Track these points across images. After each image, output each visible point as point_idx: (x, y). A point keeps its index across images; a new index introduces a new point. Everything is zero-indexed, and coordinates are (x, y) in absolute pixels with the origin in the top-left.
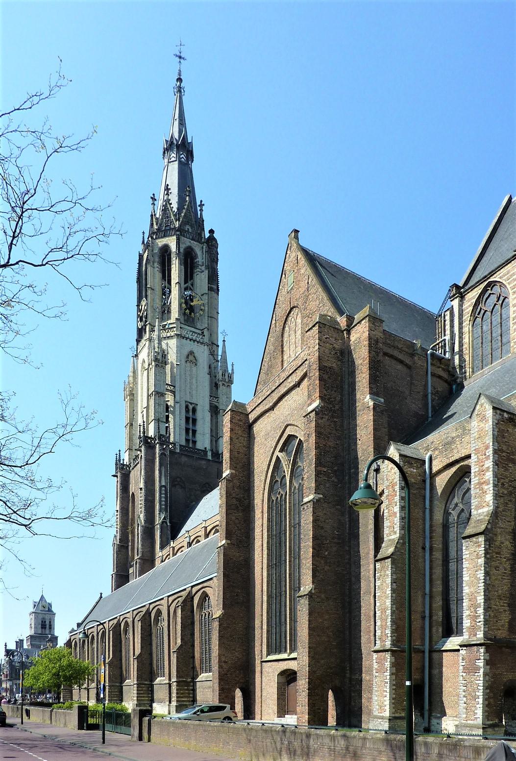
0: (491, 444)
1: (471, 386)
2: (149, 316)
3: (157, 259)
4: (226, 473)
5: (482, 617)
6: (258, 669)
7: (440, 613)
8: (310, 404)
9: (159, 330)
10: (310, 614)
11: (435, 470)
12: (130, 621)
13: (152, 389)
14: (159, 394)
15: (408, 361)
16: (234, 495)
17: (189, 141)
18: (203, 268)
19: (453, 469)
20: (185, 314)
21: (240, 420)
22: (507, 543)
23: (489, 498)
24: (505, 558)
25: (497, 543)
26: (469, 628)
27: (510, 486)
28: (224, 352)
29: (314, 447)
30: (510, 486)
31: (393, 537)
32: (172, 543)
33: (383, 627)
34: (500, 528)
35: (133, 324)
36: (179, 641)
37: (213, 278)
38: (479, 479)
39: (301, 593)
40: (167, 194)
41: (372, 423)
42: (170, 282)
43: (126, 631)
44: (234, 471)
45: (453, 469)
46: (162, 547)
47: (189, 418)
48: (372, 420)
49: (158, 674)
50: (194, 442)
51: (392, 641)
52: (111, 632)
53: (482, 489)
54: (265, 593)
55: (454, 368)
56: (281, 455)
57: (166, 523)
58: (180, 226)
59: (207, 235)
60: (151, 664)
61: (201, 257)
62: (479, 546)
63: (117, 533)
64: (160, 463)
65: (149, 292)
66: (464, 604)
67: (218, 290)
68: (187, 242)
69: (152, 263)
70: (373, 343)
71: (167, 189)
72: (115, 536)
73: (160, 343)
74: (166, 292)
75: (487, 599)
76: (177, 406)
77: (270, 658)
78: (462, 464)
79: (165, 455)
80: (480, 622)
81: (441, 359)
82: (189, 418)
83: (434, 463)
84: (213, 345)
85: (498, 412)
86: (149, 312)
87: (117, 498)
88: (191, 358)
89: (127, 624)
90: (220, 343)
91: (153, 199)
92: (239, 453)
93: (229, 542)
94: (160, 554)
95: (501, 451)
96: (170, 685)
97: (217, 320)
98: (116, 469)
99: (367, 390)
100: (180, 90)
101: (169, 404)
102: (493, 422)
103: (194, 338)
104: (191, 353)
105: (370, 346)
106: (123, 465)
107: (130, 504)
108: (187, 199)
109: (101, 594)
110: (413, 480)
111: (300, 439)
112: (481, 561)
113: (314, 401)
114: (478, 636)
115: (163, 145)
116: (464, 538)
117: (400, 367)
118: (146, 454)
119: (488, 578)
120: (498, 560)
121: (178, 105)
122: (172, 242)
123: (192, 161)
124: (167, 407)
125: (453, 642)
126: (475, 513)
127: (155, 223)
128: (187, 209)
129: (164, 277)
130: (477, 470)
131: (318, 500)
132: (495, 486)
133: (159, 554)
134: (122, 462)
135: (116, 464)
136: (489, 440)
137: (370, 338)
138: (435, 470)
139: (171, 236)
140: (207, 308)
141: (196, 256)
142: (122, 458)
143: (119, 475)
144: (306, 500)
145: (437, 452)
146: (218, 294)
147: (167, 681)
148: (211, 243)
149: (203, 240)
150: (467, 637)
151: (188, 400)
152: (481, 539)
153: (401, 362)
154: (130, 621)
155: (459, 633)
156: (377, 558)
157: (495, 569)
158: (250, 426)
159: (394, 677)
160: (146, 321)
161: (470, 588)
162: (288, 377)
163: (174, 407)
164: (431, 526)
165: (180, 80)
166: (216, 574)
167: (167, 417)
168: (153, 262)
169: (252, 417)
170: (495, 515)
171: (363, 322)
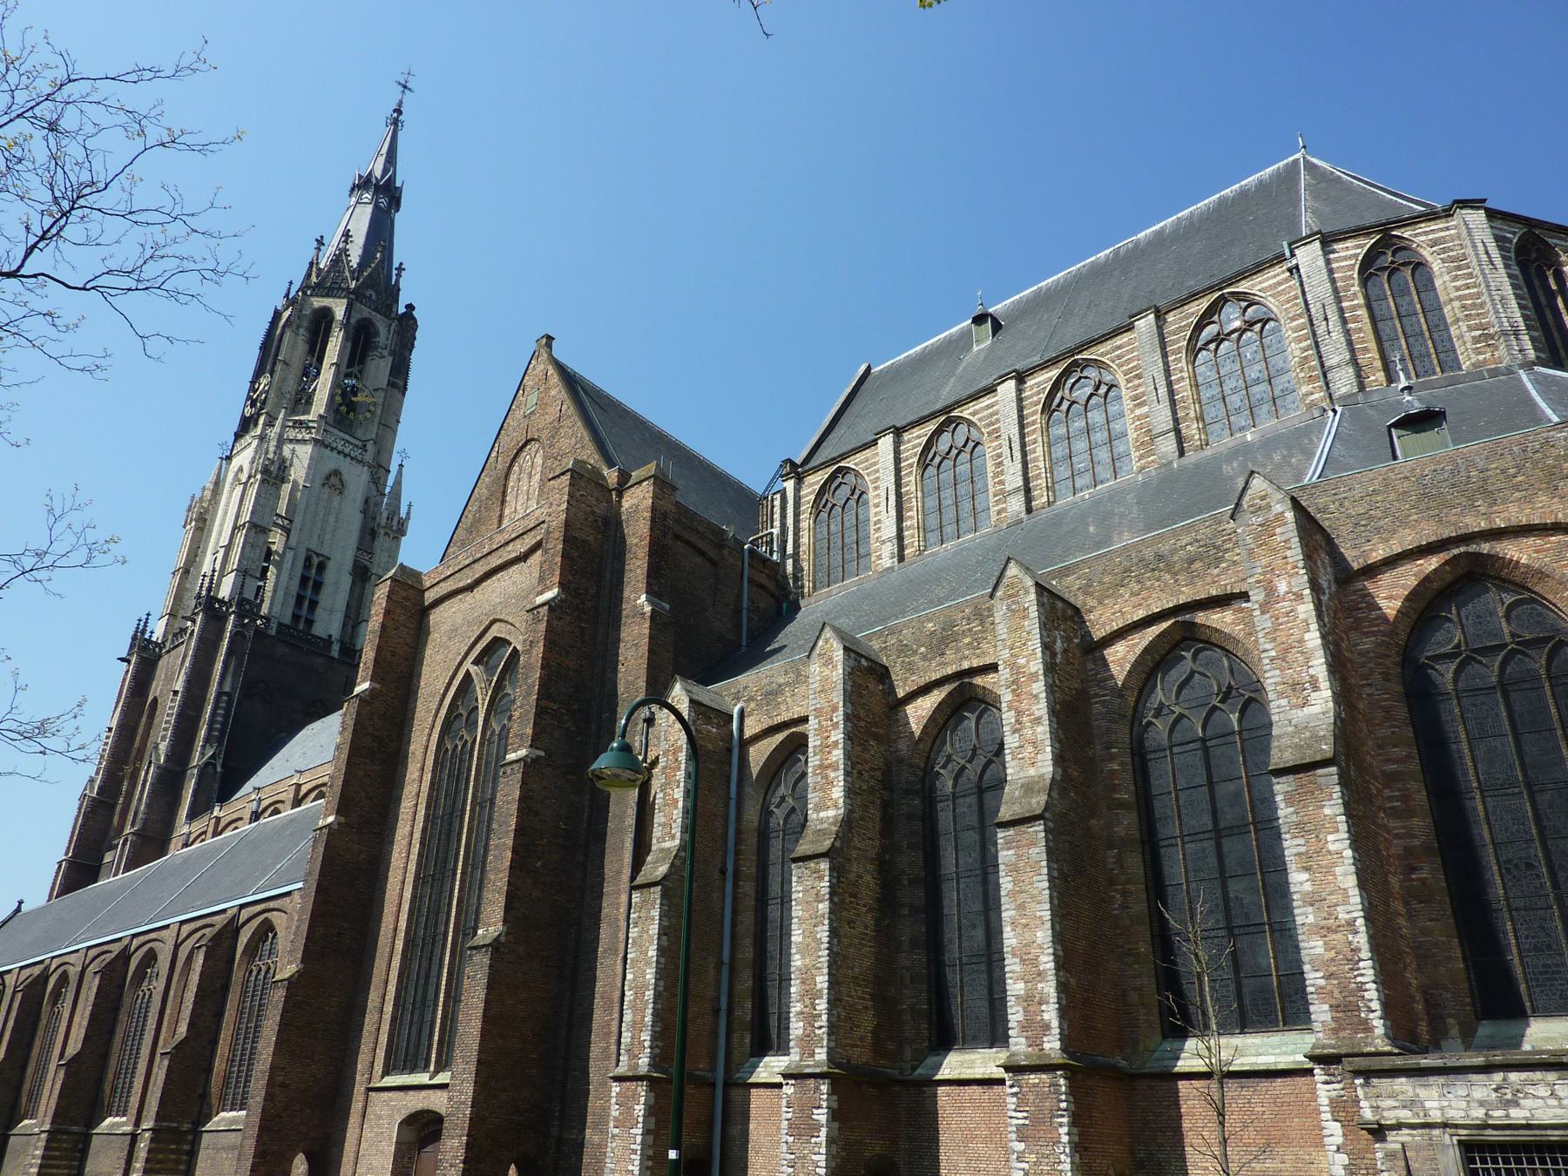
0: (841, 704)
1: (813, 607)
2: (270, 402)
3: (305, 324)
4: (362, 687)
5: (824, 1017)
6: (357, 1105)
7: (749, 1005)
8: (541, 593)
9: (284, 427)
10: (490, 987)
11: (748, 733)
12: (73, 972)
13: (246, 517)
14: (257, 528)
15: (712, 553)
16: (370, 730)
17: (398, 184)
18: (385, 353)
19: (780, 737)
20: (337, 411)
21: (405, 598)
22: (868, 878)
23: (838, 793)
24: (864, 906)
25: (852, 876)
26: (800, 1039)
27: (872, 777)
28: (398, 482)
29: (539, 664)
30: (872, 777)
31: (667, 844)
32: (217, 809)
33: (637, 1026)
34: (855, 848)
35: (236, 407)
36: (183, 1029)
37: (400, 371)
38: (821, 760)
39: (478, 941)
40: (346, 242)
41: (647, 640)
42: (320, 360)
43: (57, 995)
44: (377, 686)
45: (780, 737)
46: (193, 816)
47: (309, 578)
48: (647, 634)
49: (110, 1106)
50: (310, 622)
51: (653, 1057)
52: (19, 996)
53: (827, 777)
54: (401, 935)
55: (785, 577)
56: (474, 669)
57: (215, 766)
58: (357, 288)
59: (402, 310)
60: (100, 1081)
61: (385, 333)
62: (821, 878)
63: (97, 773)
64: (229, 648)
65: (279, 367)
66: (793, 990)
67: (406, 389)
68: (364, 312)
69: (294, 327)
70: (658, 518)
71: (347, 235)
72: (92, 781)
73: (279, 446)
74: (310, 371)
75: (834, 983)
76: (290, 554)
77: (390, 1081)
78: (794, 730)
79: (244, 636)
80: (820, 1028)
81: (765, 561)
82: (309, 578)
83: (748, 721)
84: (379, 469)
85: (852, 655)
86: (272, 395)
87: (117, 703)
88: (334, 480)
89: (64, 978)
90: (394, 468)
92: (393, 654)
93: (342, 820)
94: (185, 830)
95: (859, 718)
96: (134, 1138)
97: (395, 432)
98: (132, 646)
99: (643, 586)
100: (396, 122)
101: (274, 548)
102: (844, 670)
103: (347, 451)
104: (336, 473)
105: (653, 519)
106: (149, 641)
107: (144, 719)
108: (378, 255)
109: (21, 903)
110: (710, 746)
111: (515, 647)
112: (824, 907)
113: (549, 588)
114: (817, 1057)
115: (352, 178)
116: (795, 860)
117: (699, 560)
118: (203, 630)
119: (835, 941)
120: (854, 909)
121: (388, 139)
122: (339, 308)
123: (397, 210)
124: (269, 553)
125: (770, 1067)
126: (815, 816)
127: (314, 274)
128: (375, 269)
129: (311, 351)
130: (818, 743)
131: (536, 761)
132: (847, 774)
133: (182, 828)
134: (147, 636)
135: (134, 638)
136: (838, 698)
137: (654, 509)
138: (748, 733)
139: (339, 297)
140: (379, 411)
141: (377, 334)
142: (149, 629)
143: (134, 660)
144: (511, 756)
145: (753, 705)
146: (404, 395)
147: (128, 1129)
148: (407, 324)
149: (393, 315)
150: (798, 1058)
151: (313, 547)
152: (824, 865)
153: (702, 553)
154: (73, 972)
155: (783, 1049)
156: (636, 883)
157: (849, 924)
158: (424, 612)
159: (650, 1139)
160: (262, 409)
161: (803, 957)
162: (507, 543)
163: (282, 556)
164: (738, 832)
166: (300, 885)
167: (265, 570)
168: (298, 327)
169: (430, 597)
170: (848, 824)
171: (645, 484)
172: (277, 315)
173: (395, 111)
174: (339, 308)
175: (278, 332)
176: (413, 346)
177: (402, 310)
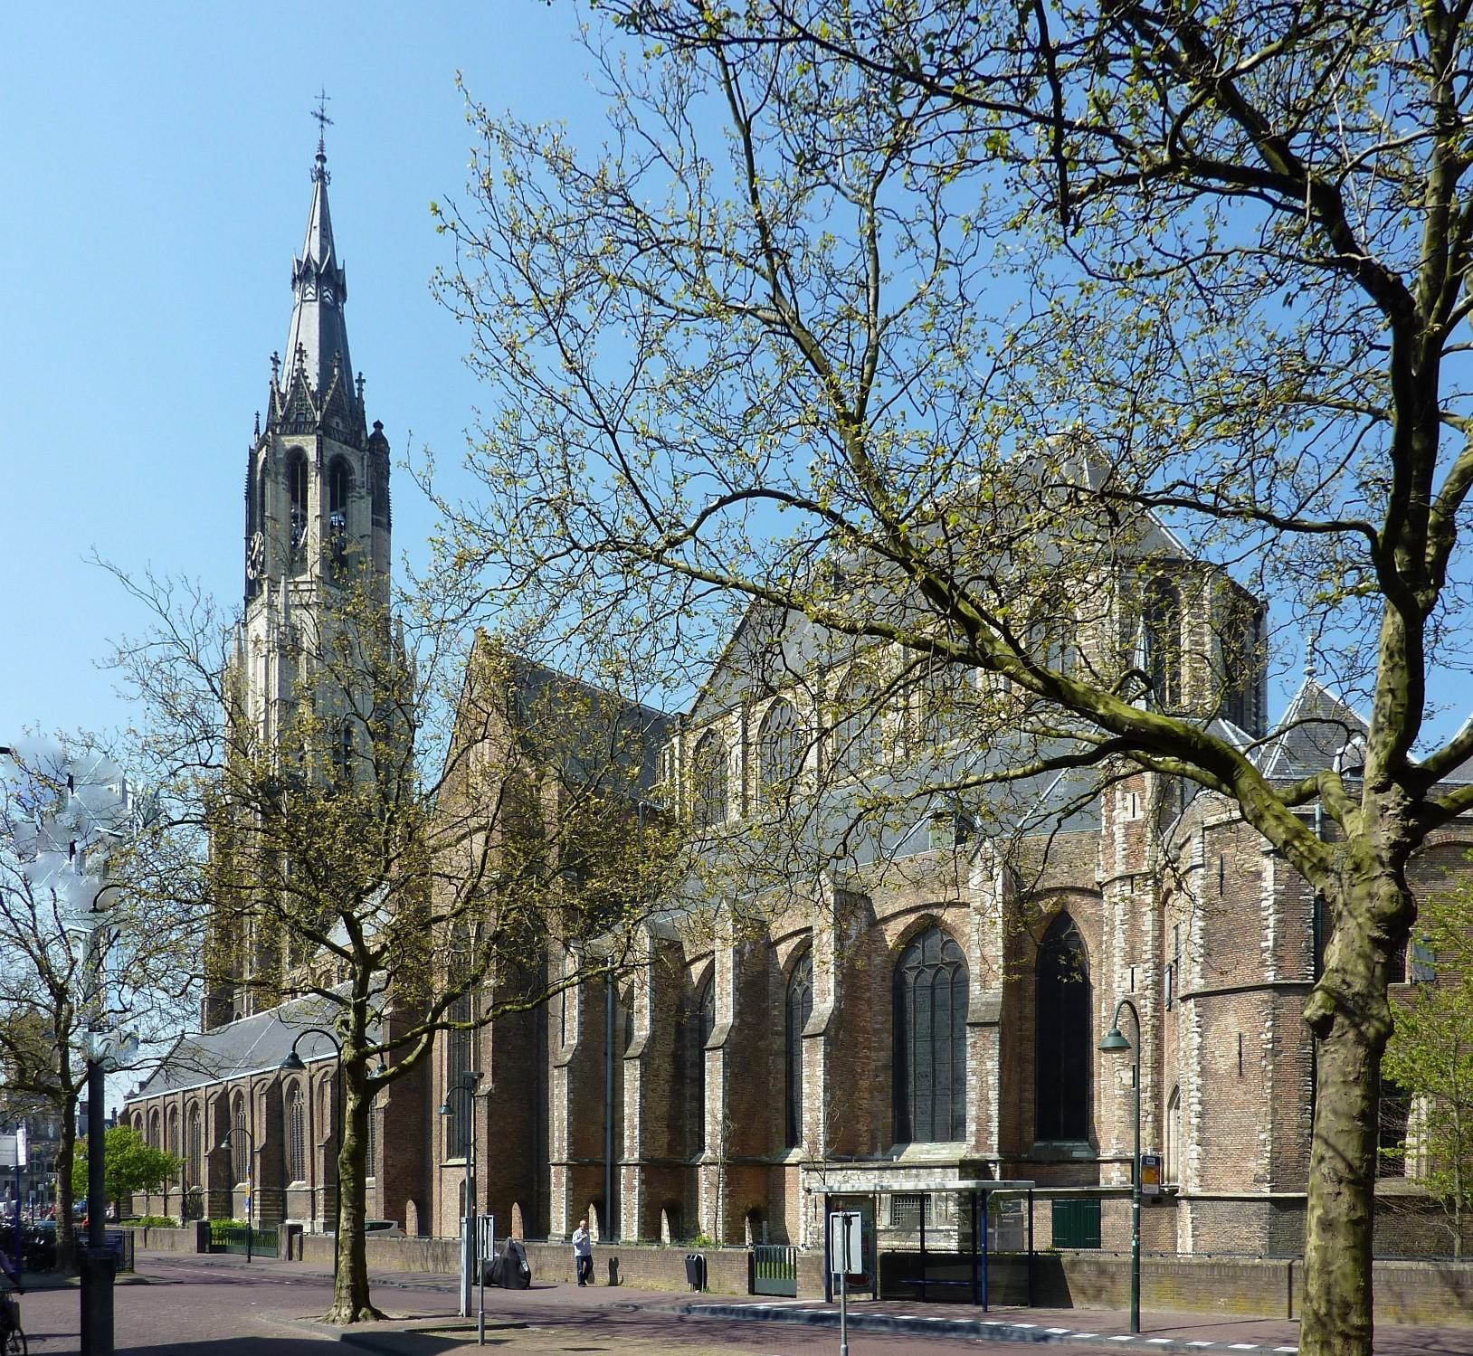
2: (268, 565)
3: (282, 470)
9: (287, 592)
12: (246, 1091)
13: (274, 695)
17: (339, 267)
18: (363, 492)
36: (328, 1131)
40: (301, 360)
42: (305, 507)
43: (237, 1106)
59: (371, 430)
65: (269, 524)
67: (390, 525)
68: (336, 447)
71: (300, 351)
73: (287, 617)
86: (268, 558)
89: (239, 1095)
100: (321, 176)
115: (289, 270)
121: (318, 203)
122: (309, 445)
123: (345, 300)
127: (278, 406)
128: (336, 390)
129: (294, 499)
139: (308, 434)
141: (351, 471)
154: (246, 1091)
168: (277, 474)
172: (253, 457)
174: (309, 445)
175: (258, 478)
176: (389, 473)
177: (371, 430)
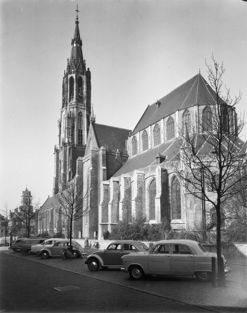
47: (80, 135)
59: (87, 70)
61: (84, 78)
82: (80, 135)
91: (68, 60)
98: (55, 151)
106: (57, 150)
109: (49, 196)
134: (57, 149)
135: (55, 149)
142: (57, 148)
148: (88, 75)
165: (77, 19)
173: (76, 19)
177: (87, 70)
